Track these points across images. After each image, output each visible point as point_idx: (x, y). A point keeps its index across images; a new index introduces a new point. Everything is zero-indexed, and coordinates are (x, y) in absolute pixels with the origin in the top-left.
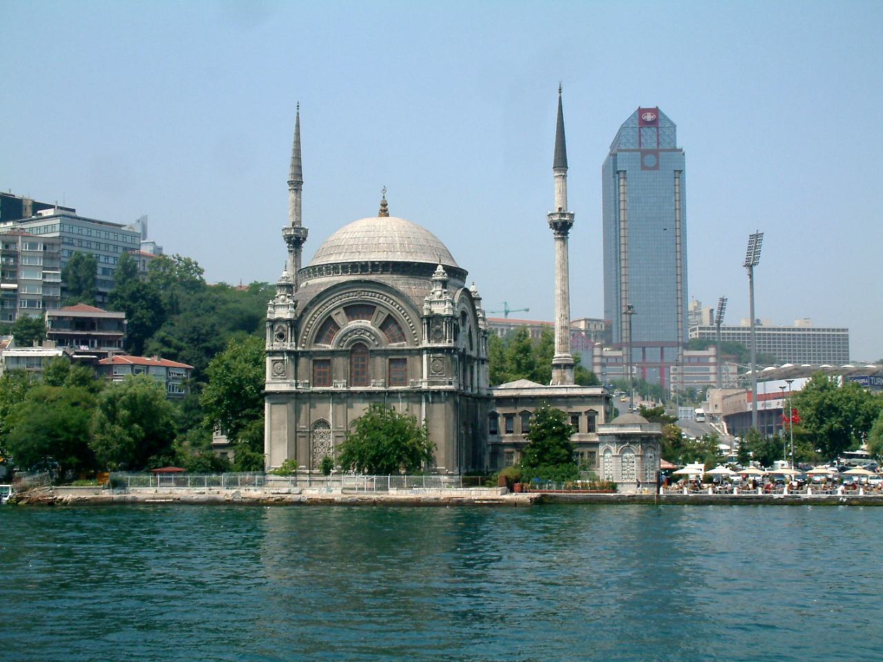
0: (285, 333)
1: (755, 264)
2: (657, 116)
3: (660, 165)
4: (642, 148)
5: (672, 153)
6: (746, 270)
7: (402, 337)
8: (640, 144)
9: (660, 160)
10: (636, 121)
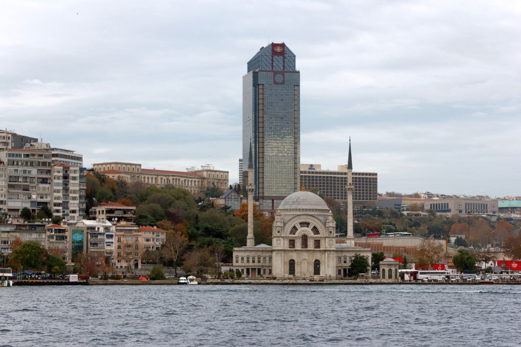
2: (284, 49)
3: (285, 81)
4: (274, 69)
7: (319, 234)
10: (271, 52)
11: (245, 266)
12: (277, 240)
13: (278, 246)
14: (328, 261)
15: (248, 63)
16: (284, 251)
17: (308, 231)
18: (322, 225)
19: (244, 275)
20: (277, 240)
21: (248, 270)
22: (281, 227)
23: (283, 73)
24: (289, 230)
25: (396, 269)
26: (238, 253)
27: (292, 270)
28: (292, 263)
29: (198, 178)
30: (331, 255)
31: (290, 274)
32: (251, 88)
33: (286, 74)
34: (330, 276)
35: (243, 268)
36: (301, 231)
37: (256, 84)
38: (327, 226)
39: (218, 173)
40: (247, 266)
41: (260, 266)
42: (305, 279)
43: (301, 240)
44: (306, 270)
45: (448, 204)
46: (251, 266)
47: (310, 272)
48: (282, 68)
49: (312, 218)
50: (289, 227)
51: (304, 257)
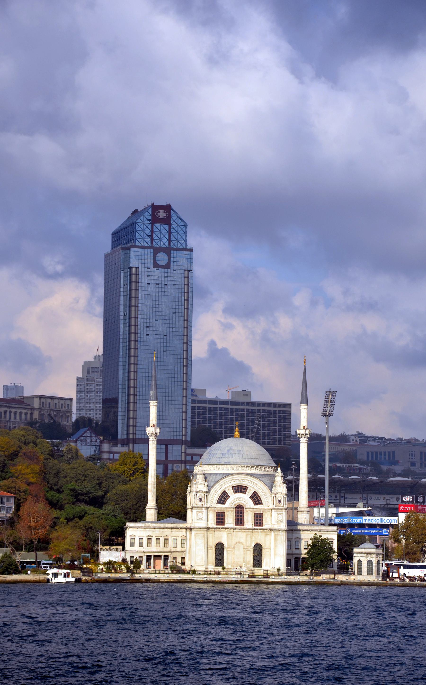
0: (203, 499)
1: (330, 415)
5: (184, 252)
8: (152, 240)
9: (172, 259)
11: (144, 552)
12: (199, 512)
13: (200, 521)
14: (275, 546)
15: (113, 234)
16: (208, 529)
17: (245, 499)
19: (143, 566)
20: (198, 513)
21: (149, 558)
23: (167, 251)
25: (378, 561)
26: (133, 531)
27: (220, 560)
28: (220, 549)
29: (25, 409)
30: (279, 537)
31: (217, 564)
33: (172, 252)
34: (279, 570)
35: (141, 555)
36: (234, 499)
38: (274, 491)
39: (56, 401)
40: (148, 552)
41: (168, 552)
42: (240, 574)
44: (242, 560)
45: (394, 453)
46: (155, 552)
47: (247, 563)
48: (167, 243)
49: (251, 478)
51: (238, 540)
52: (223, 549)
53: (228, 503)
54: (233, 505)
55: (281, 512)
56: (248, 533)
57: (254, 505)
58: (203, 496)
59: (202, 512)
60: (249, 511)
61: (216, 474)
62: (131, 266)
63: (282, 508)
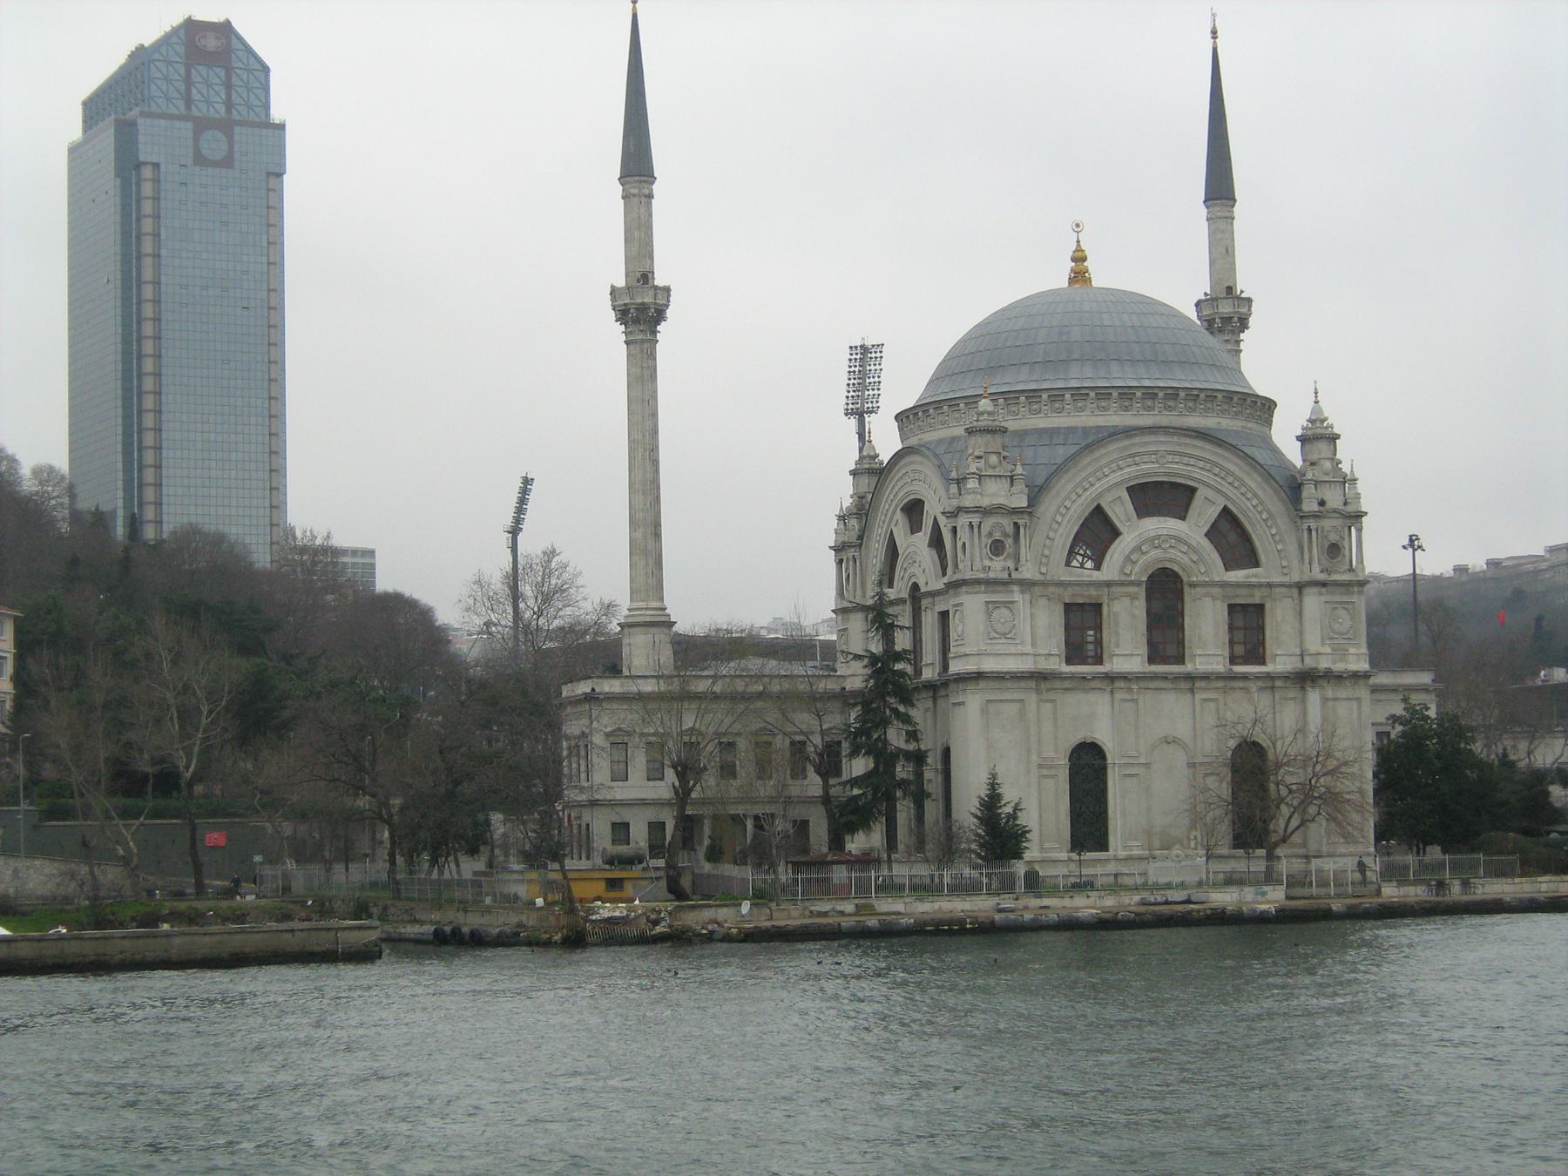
3: (237, 156)
5: (264, 132)
6: (853, 422)
7: (1257, 564)
8: (189, 102)
10: (181, 49)
12: (997, 605)
15: (85, 104)
16: (1040, 677)
18: (1275, 504)
22: (1015, 511)
23: (226, 127)
24: (1064, 534)
28: (1088, 764)
32: (109, 182)
33: (237, 129)
36: (1142, 539)
37: (128, 165)
38: (1309, 506)
43: (1140, 608)
48: (222, 109)
50: (1062, 516)
52: (1103, 769)
53: (1112, 566)
54: (1139, 572)
55: (1346, 599)
56: (1206, 696)
57: (1227, 570)
58: (1010, 529)
59: (1008, 605)
60: (1207, 595)
61: (1052, 432)
62: (142, 159)
63: (1346, 577)
